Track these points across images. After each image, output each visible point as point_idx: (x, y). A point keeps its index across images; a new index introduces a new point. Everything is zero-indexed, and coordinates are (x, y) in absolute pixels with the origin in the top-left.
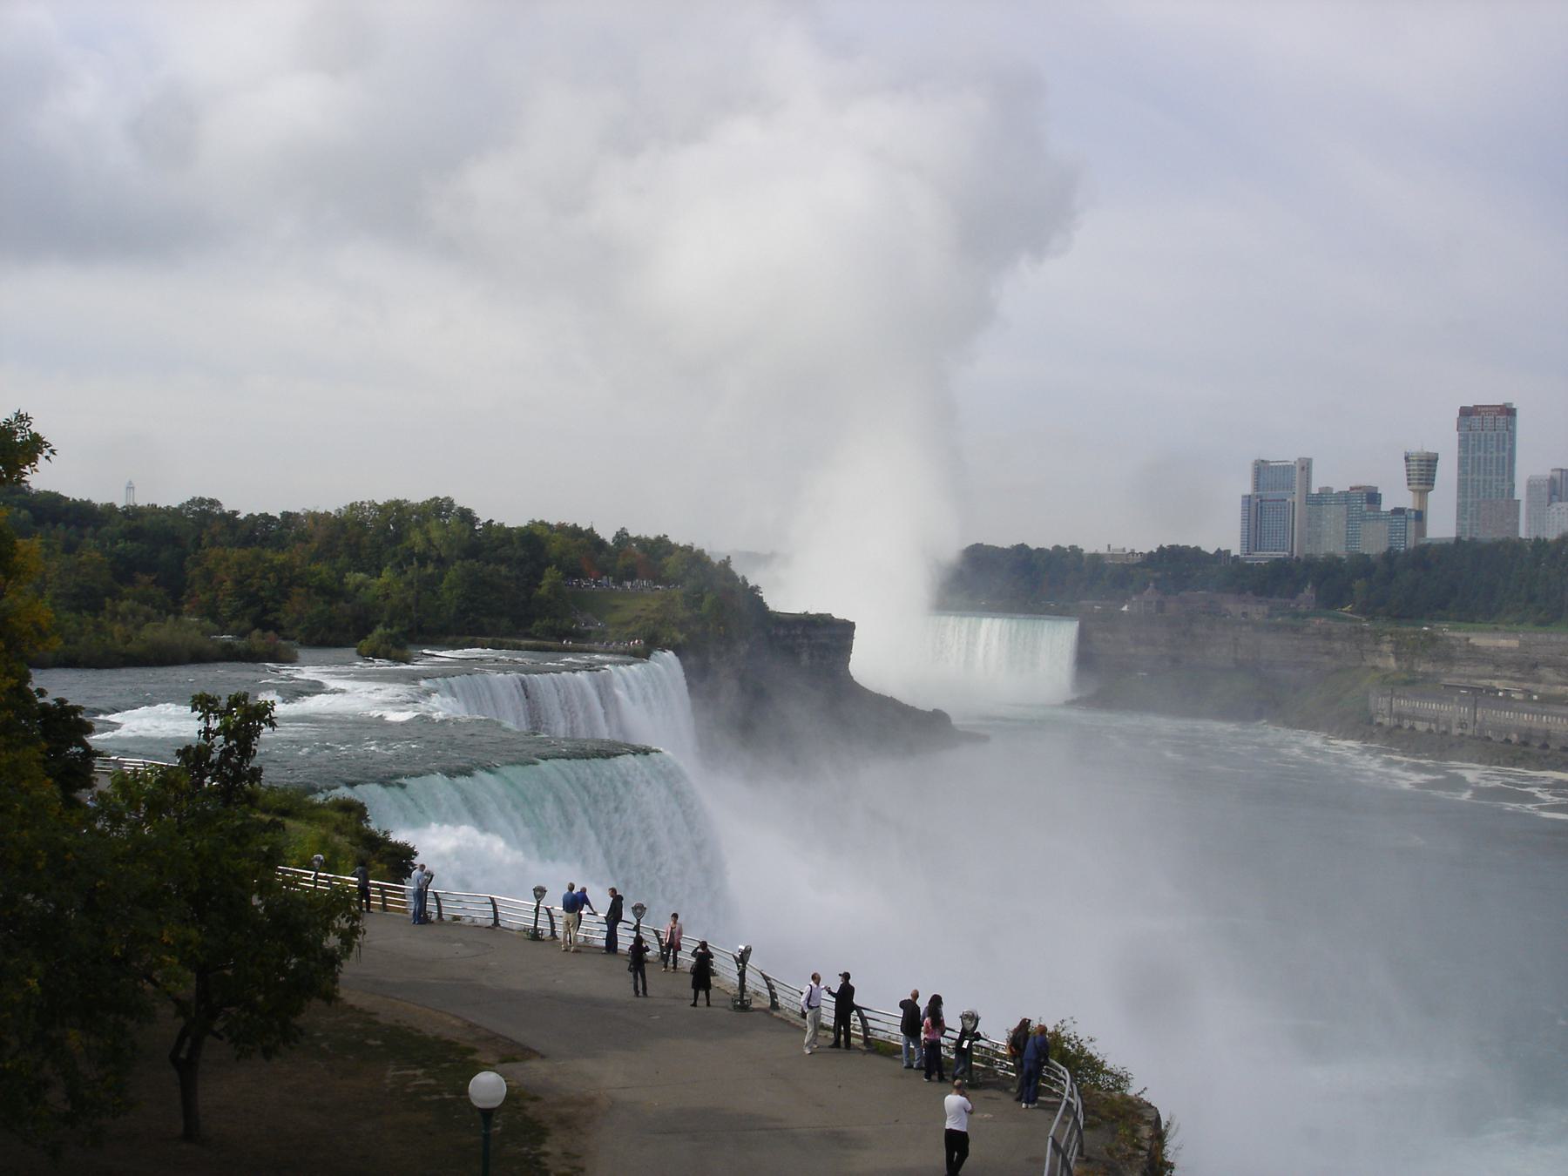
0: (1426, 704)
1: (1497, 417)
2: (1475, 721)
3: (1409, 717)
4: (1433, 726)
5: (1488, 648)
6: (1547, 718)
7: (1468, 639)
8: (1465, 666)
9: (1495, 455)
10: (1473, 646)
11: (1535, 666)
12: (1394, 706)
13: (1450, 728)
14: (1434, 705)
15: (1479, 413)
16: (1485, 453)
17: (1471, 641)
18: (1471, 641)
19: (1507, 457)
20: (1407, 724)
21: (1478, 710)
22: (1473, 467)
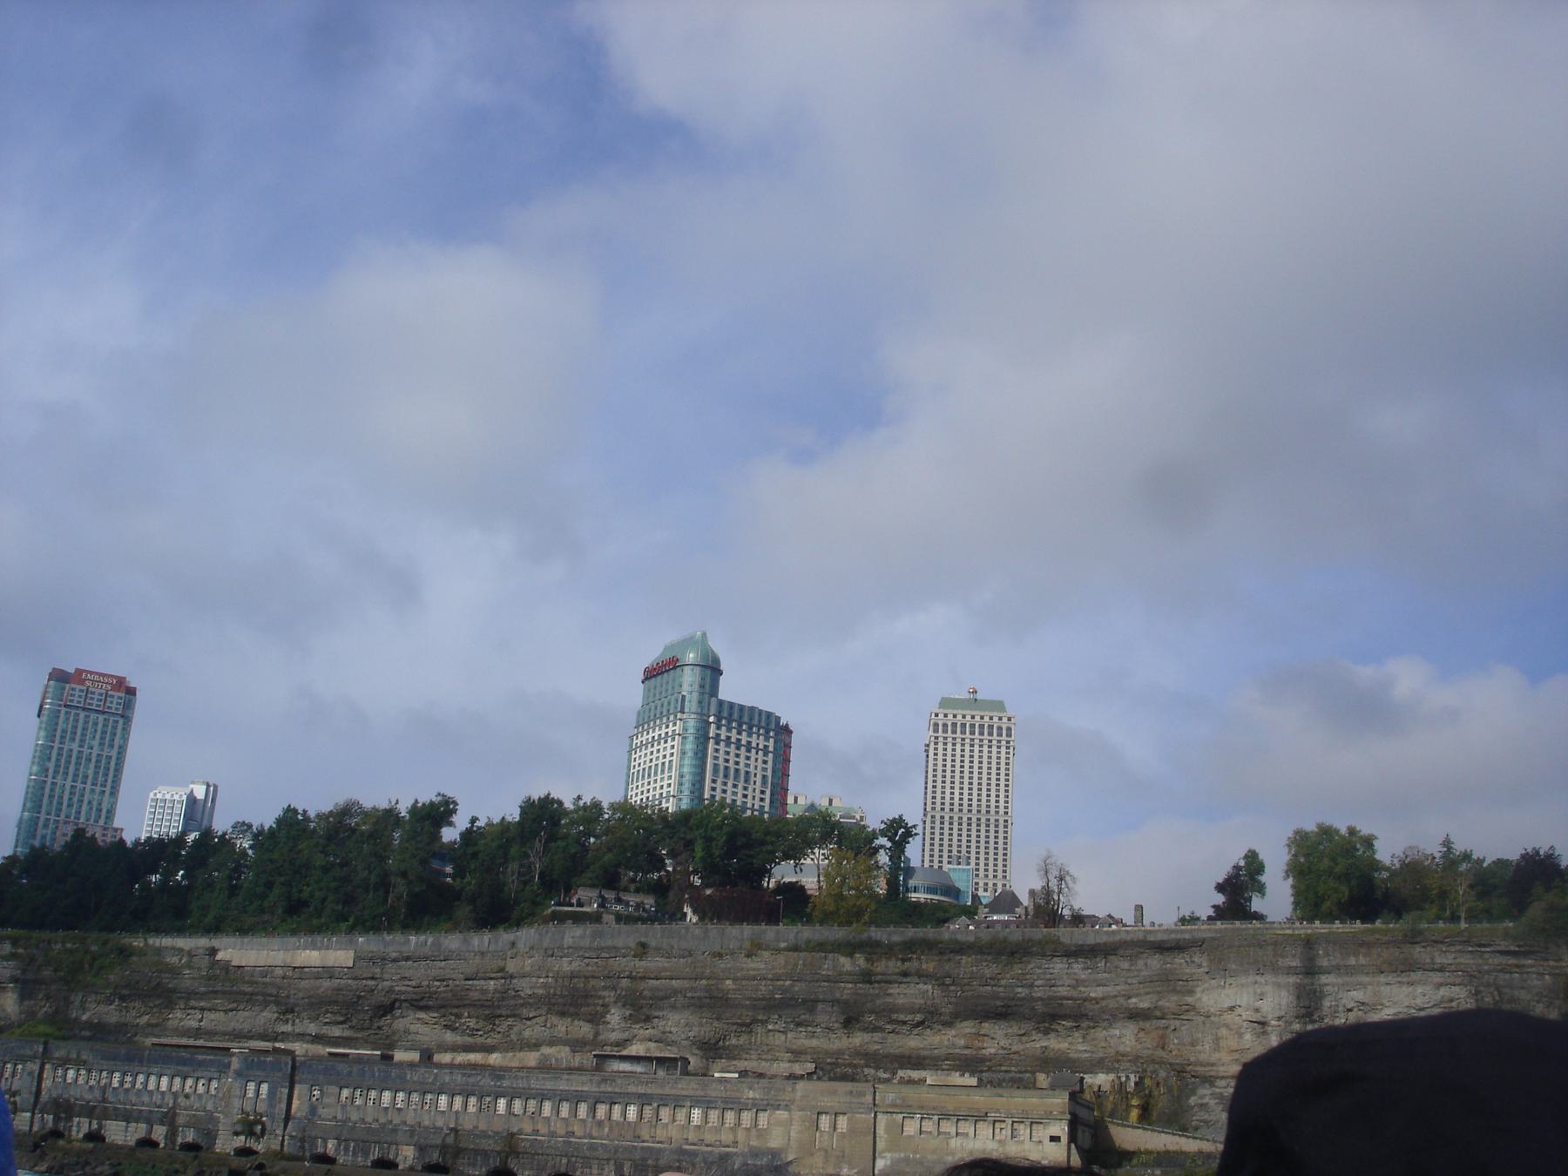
0: (141, 1078)
1: (109, 693)
2: (288, 1117)
3: (89, 1112)
4: (159, 1133)
5: (267, 970)
6: (509, 1105)
7: (213, 952)
8: (202, 1009)
9: (95, 751)
10: (226, 966)
11: (387, 1009)
12: (47, 1084)
13: (211, 1136)
14: (165, 1081)
15: (82, 682)
16: (83, 741)
17: (219, 956)
18: (219, 956)
19: (114, 759)
20: (80, 1127)
21: (297, 1088)
22: (58, 766)
